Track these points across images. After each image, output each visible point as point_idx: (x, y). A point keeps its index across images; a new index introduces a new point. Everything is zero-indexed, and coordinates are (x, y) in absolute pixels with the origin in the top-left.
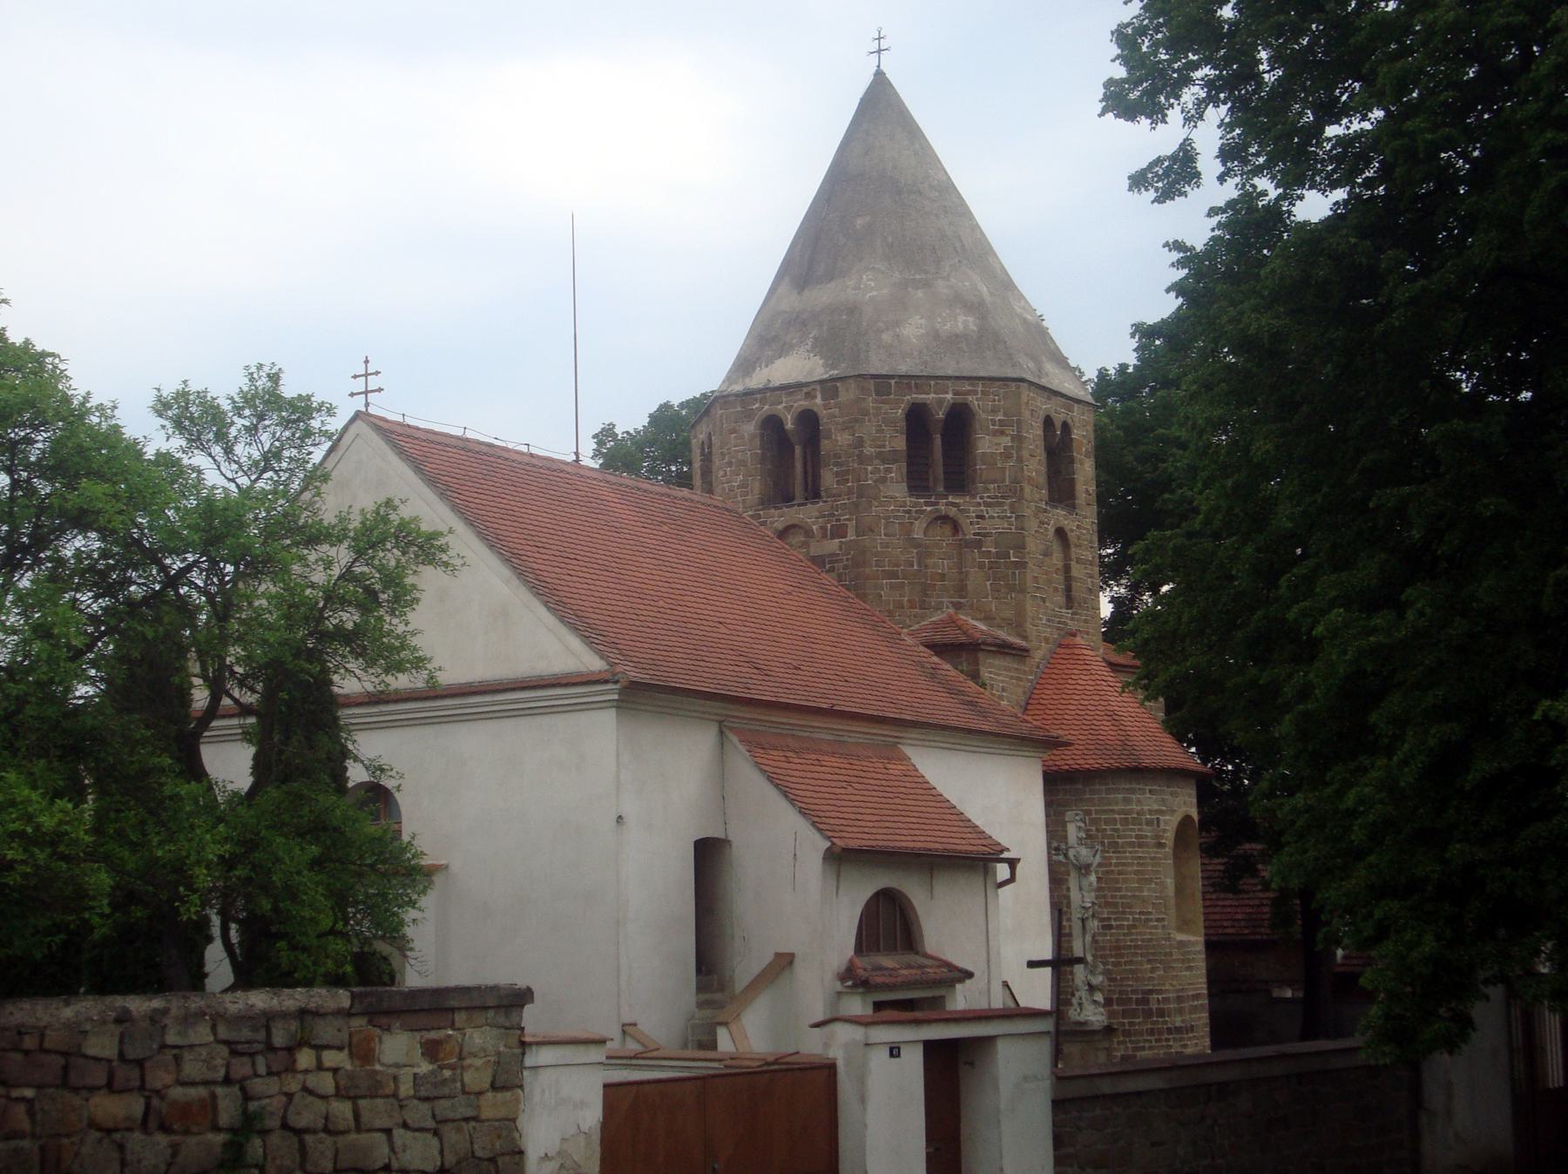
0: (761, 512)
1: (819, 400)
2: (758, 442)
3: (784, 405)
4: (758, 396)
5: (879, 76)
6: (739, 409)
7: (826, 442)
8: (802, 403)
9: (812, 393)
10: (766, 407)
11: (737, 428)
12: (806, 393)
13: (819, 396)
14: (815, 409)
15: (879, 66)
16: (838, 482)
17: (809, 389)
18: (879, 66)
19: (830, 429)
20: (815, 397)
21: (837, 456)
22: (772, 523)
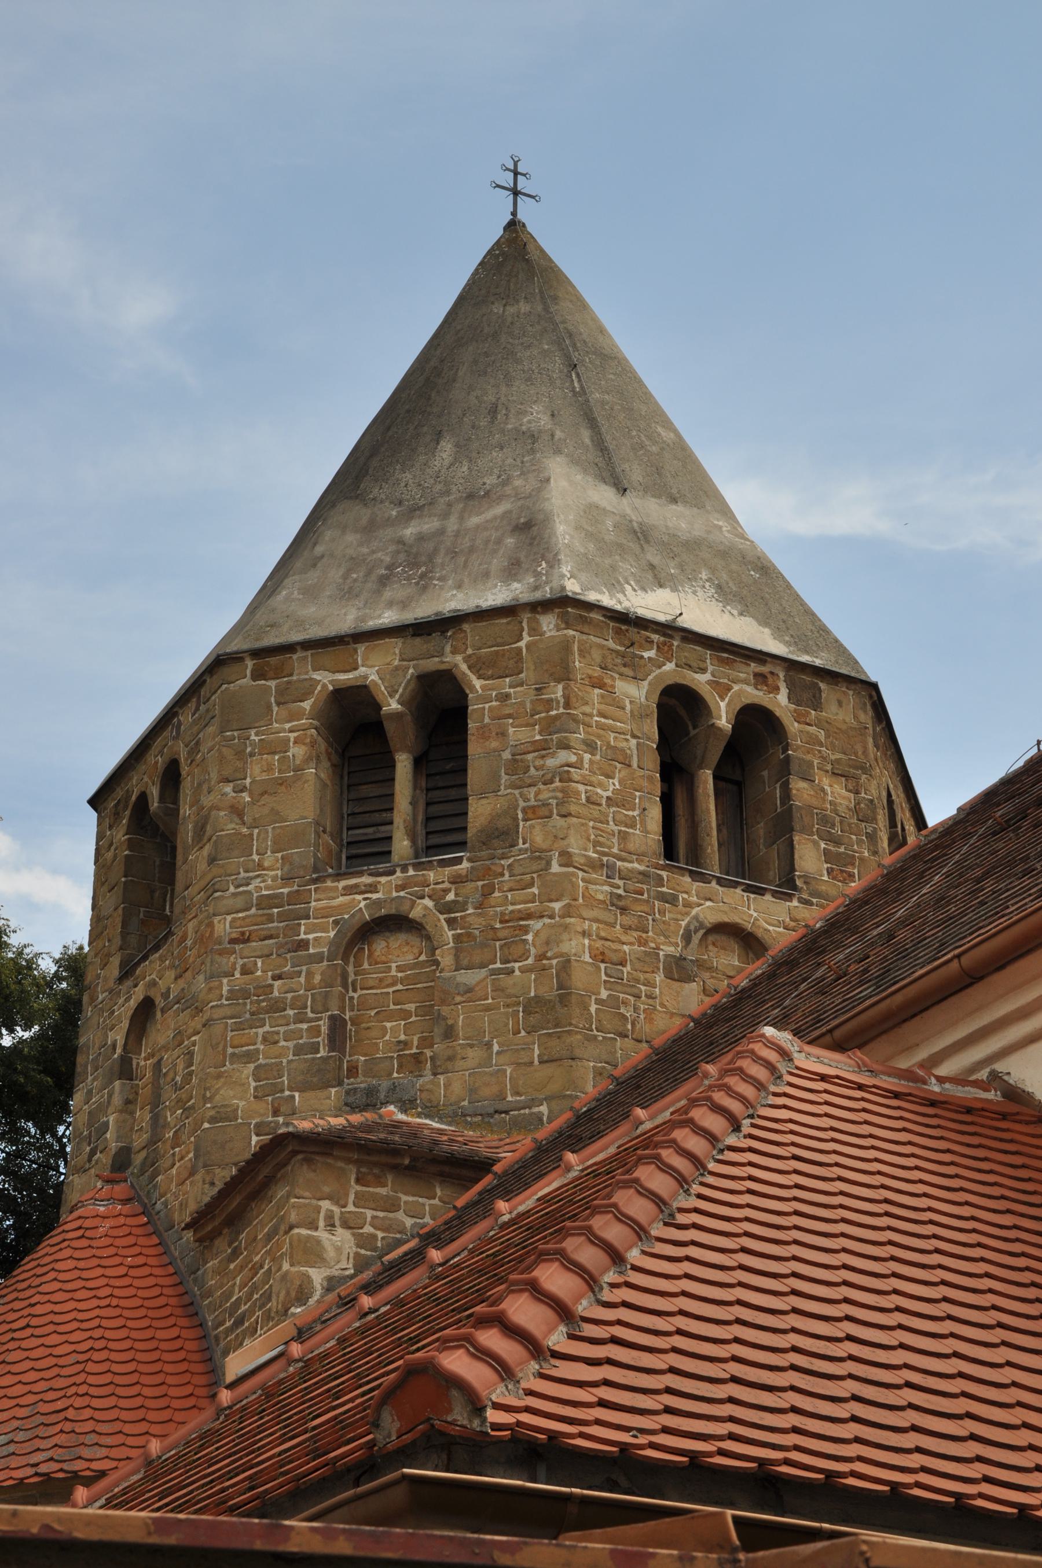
0: (664, 874)
1: (782, 697)
2: (651, 728)
3: (707, 676)
4: (655, 637)
5: (514, 226)
6: (611, 644)
7: (802, 785)
8: (749, 689)
9: (770, 681)
10: (670, 666)
11: (608, 681)
12: (756, 675)
13: (784, 692)
14: (778, 713)
15: (514, 213)
16: (830, 871)
17: (764, 669)
18: (514, 213)
19: (810, 765)
20: (777, 689)
21: (825, 820)
22: (688, 905)
